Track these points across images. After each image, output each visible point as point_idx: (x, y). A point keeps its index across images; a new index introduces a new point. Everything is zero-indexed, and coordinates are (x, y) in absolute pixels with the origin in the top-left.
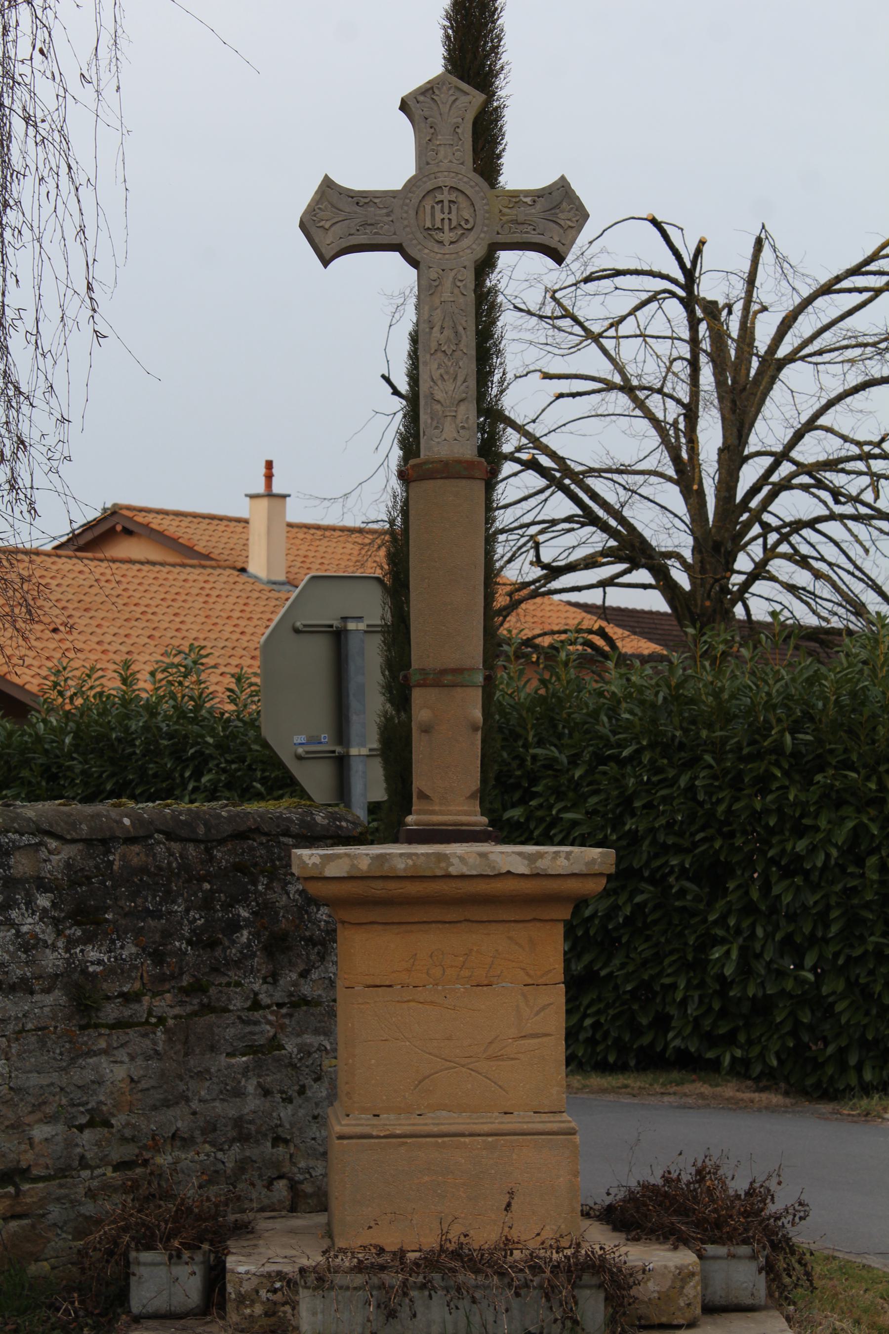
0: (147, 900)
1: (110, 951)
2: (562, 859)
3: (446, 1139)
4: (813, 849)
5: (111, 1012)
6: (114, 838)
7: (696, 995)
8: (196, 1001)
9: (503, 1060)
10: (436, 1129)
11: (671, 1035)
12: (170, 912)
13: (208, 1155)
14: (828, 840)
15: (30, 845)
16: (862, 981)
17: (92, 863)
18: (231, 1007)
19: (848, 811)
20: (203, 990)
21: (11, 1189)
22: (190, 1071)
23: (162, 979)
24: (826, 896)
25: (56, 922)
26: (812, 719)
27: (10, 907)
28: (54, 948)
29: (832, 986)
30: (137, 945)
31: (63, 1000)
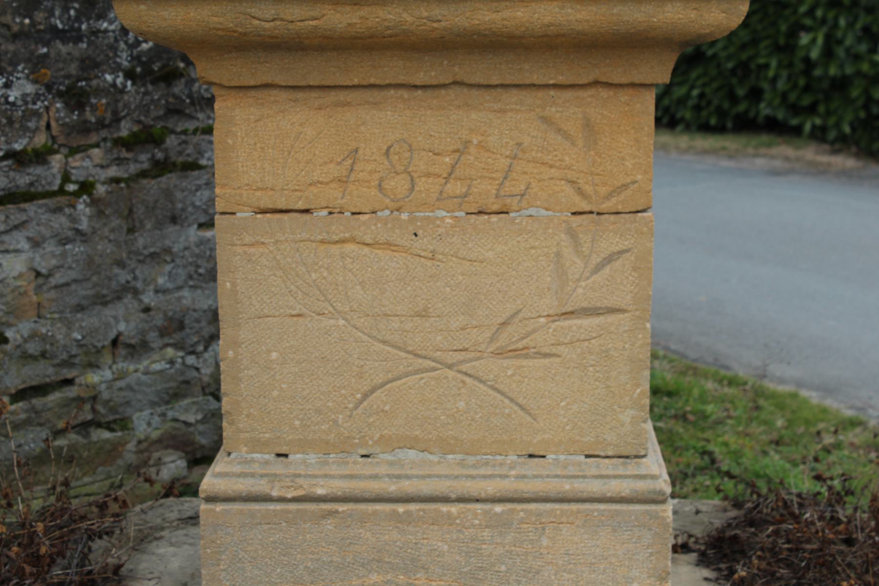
3: (413, 507)
7: (784, 73)
8: (144, 157)
9: (526, 356)
10: (392, 488)
11: (762, 105)
12: (96, 32)
13: (172, 362)
18: (203, 162)
20: (157, 141)
22: (138, 253)
23: (85, 128)
30: (35, 82)
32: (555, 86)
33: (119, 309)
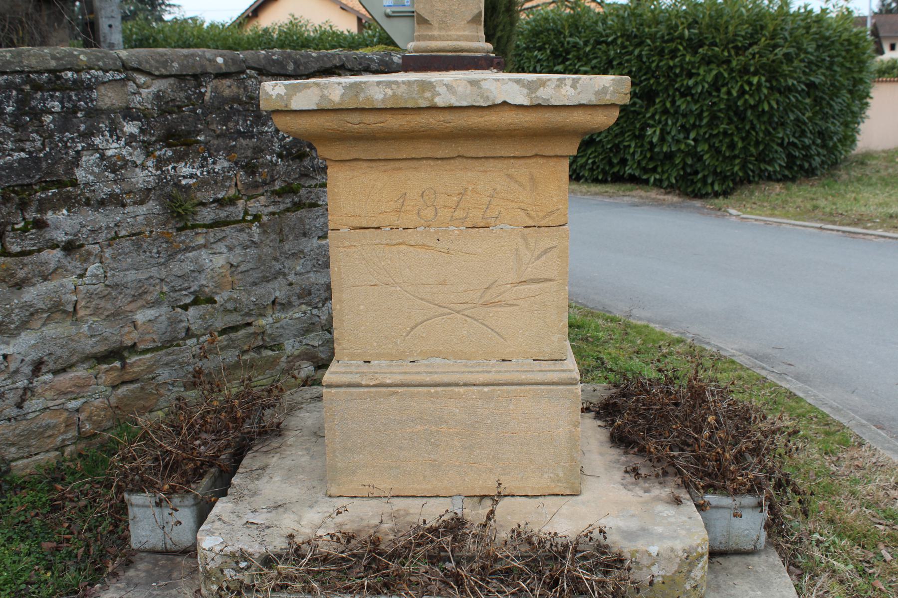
0: (238, 124)
1: (203, 167)
2: (568, 87)
3: (439, 389)
4: (696, 84)
5: (207, 215)
6: (205, 74)
7: (639, 150)
8: (288, 201)
9: (500, 306)
10: (428, 379)
11: (627, 168)
12: (261, 133)
13: (305, 313)
14: (704, 80)
15: (115, 80)
16: (717, 145)
17: (182, 95)
18: (320, 203)
19: (713, 66)
20: (295, 192)
21: (118, 364)
23: (256, 185)
24: (701, 106)
25: (147, 147)
26: (697, 22)
27: (93, 134)
28: (143, 167)
29: (703, 147)
31: (157, 209)
32: (514, 157)
33: (275, 284)
